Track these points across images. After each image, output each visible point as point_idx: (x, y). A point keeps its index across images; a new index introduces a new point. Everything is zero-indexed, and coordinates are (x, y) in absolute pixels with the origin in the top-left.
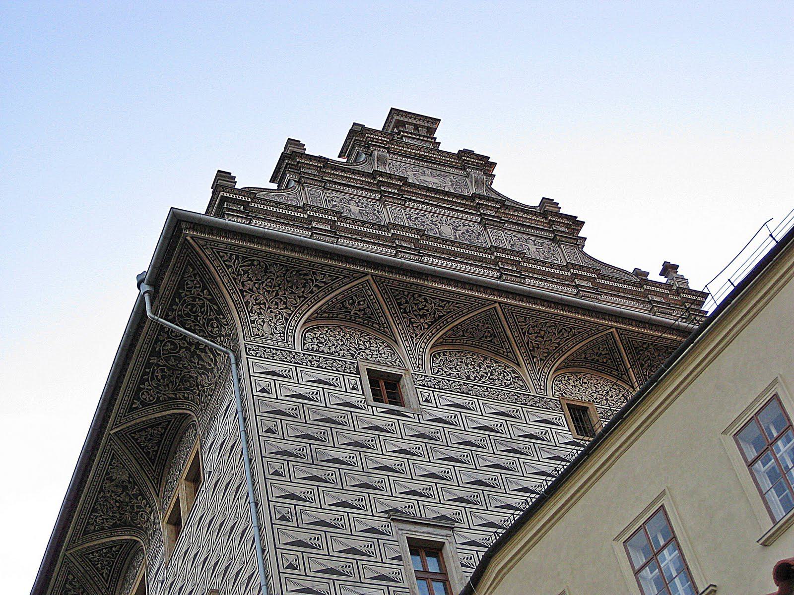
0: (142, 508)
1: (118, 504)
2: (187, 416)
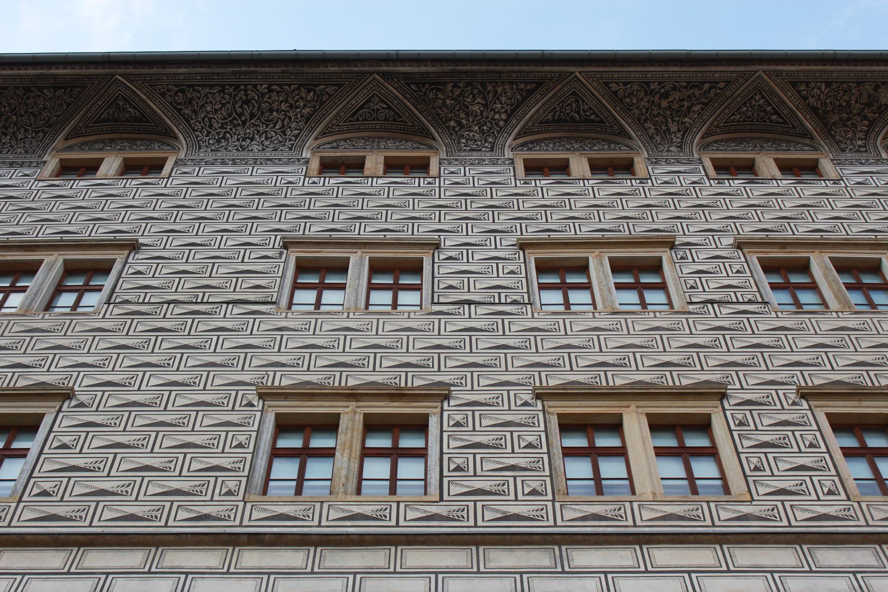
0: (856, 128)
1: (844, 104)
2: (176, 138)
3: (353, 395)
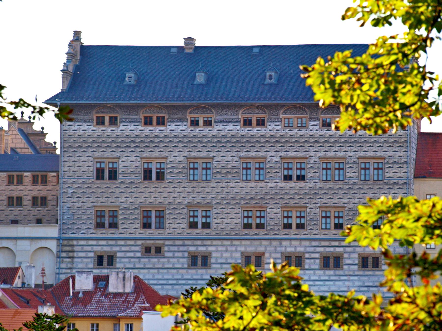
3: (254, 207)
